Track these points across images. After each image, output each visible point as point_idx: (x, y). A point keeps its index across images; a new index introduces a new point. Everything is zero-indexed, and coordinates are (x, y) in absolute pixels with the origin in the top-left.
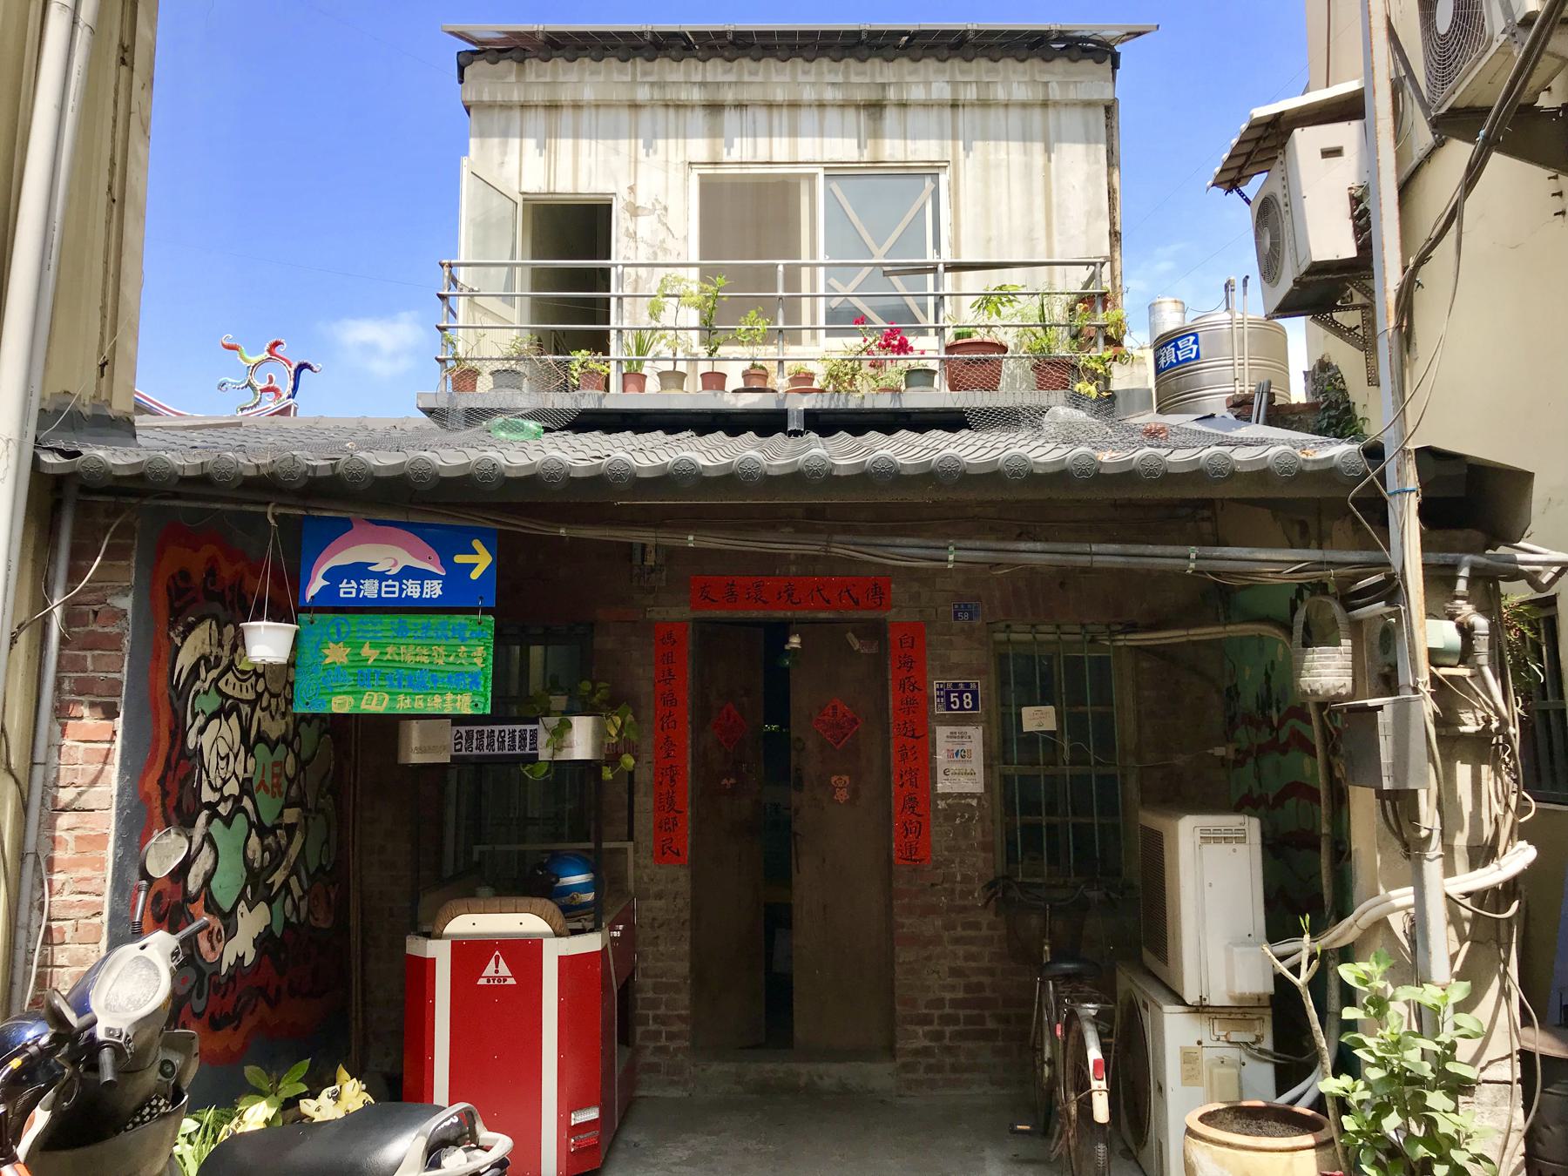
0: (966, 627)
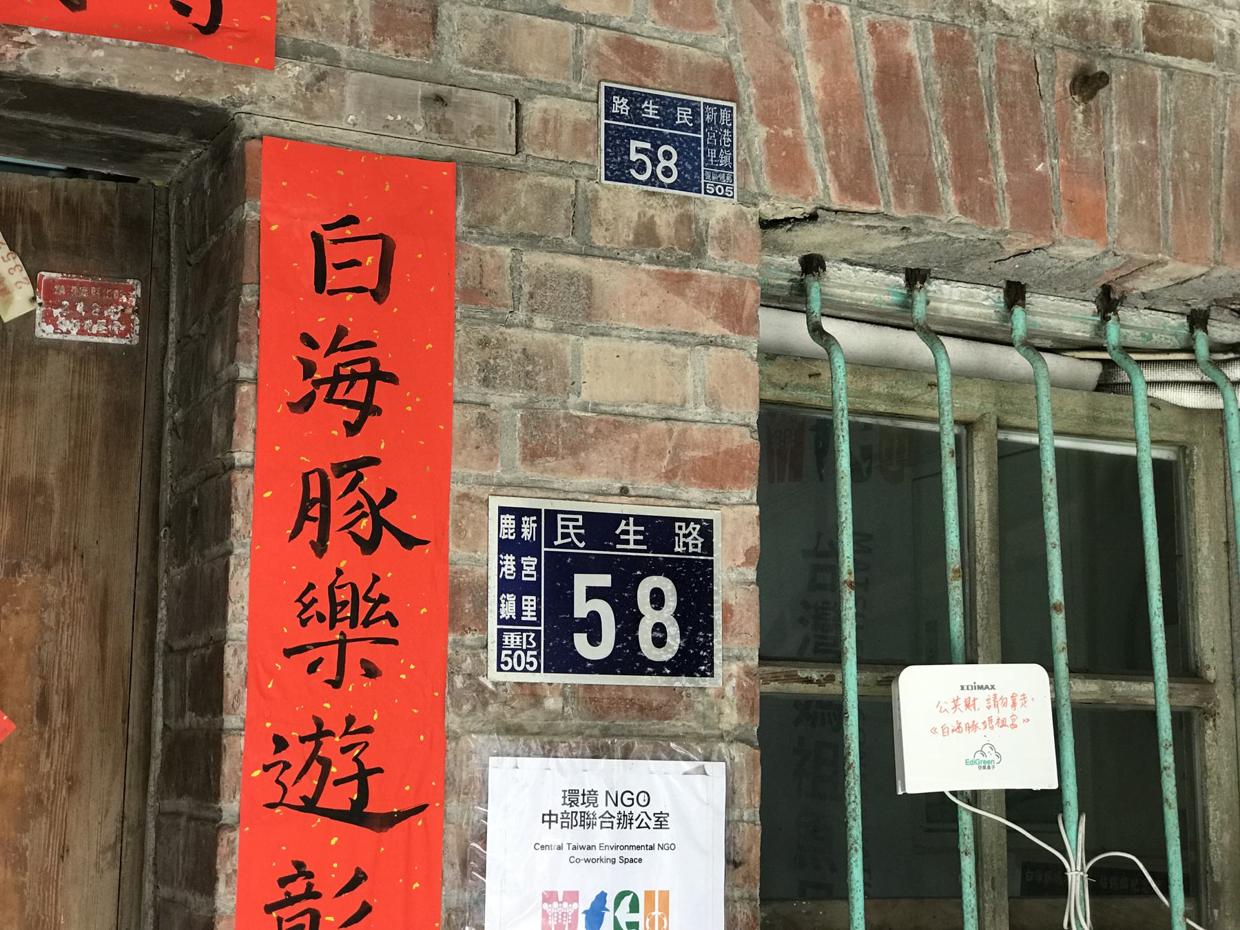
0: (665, 221)
